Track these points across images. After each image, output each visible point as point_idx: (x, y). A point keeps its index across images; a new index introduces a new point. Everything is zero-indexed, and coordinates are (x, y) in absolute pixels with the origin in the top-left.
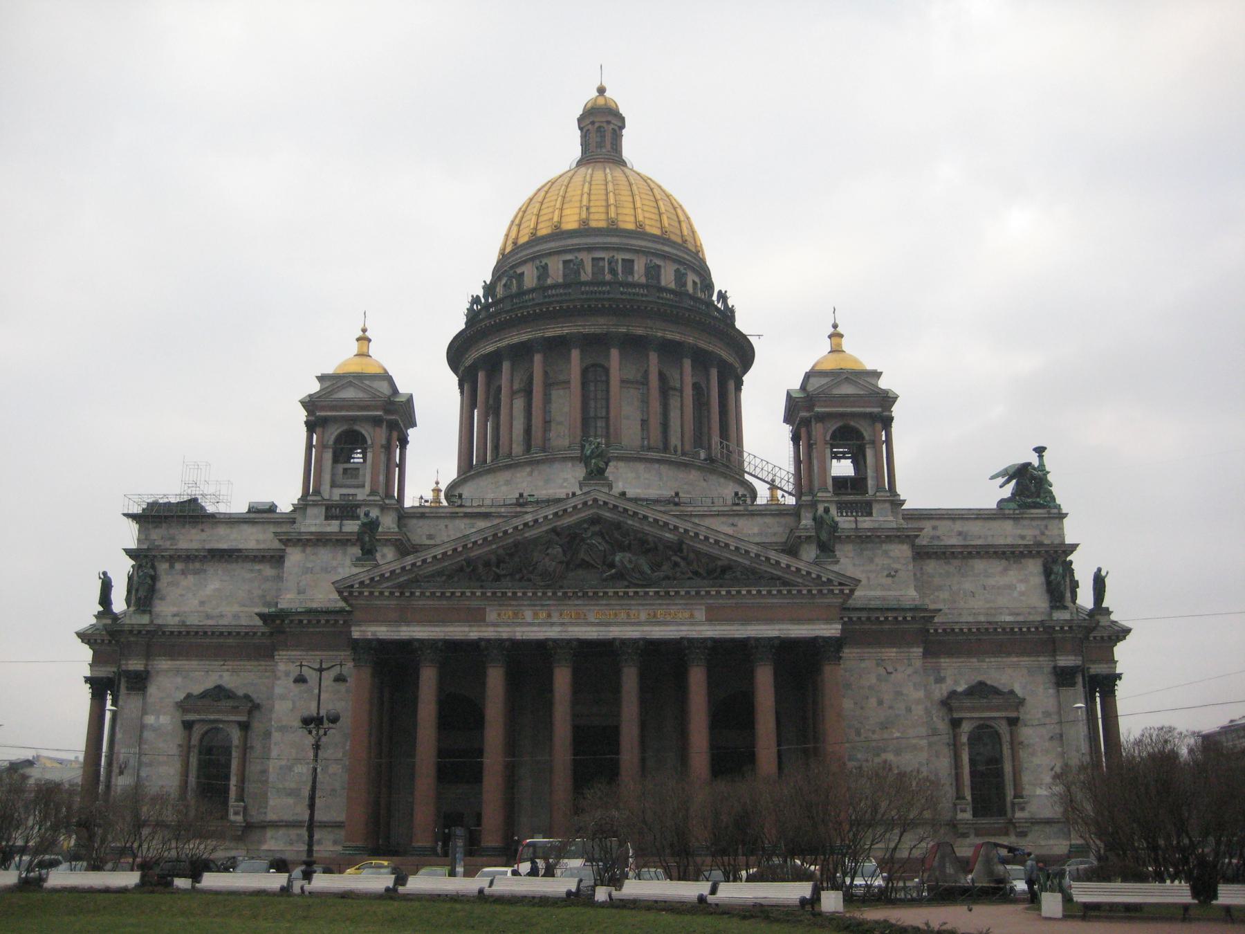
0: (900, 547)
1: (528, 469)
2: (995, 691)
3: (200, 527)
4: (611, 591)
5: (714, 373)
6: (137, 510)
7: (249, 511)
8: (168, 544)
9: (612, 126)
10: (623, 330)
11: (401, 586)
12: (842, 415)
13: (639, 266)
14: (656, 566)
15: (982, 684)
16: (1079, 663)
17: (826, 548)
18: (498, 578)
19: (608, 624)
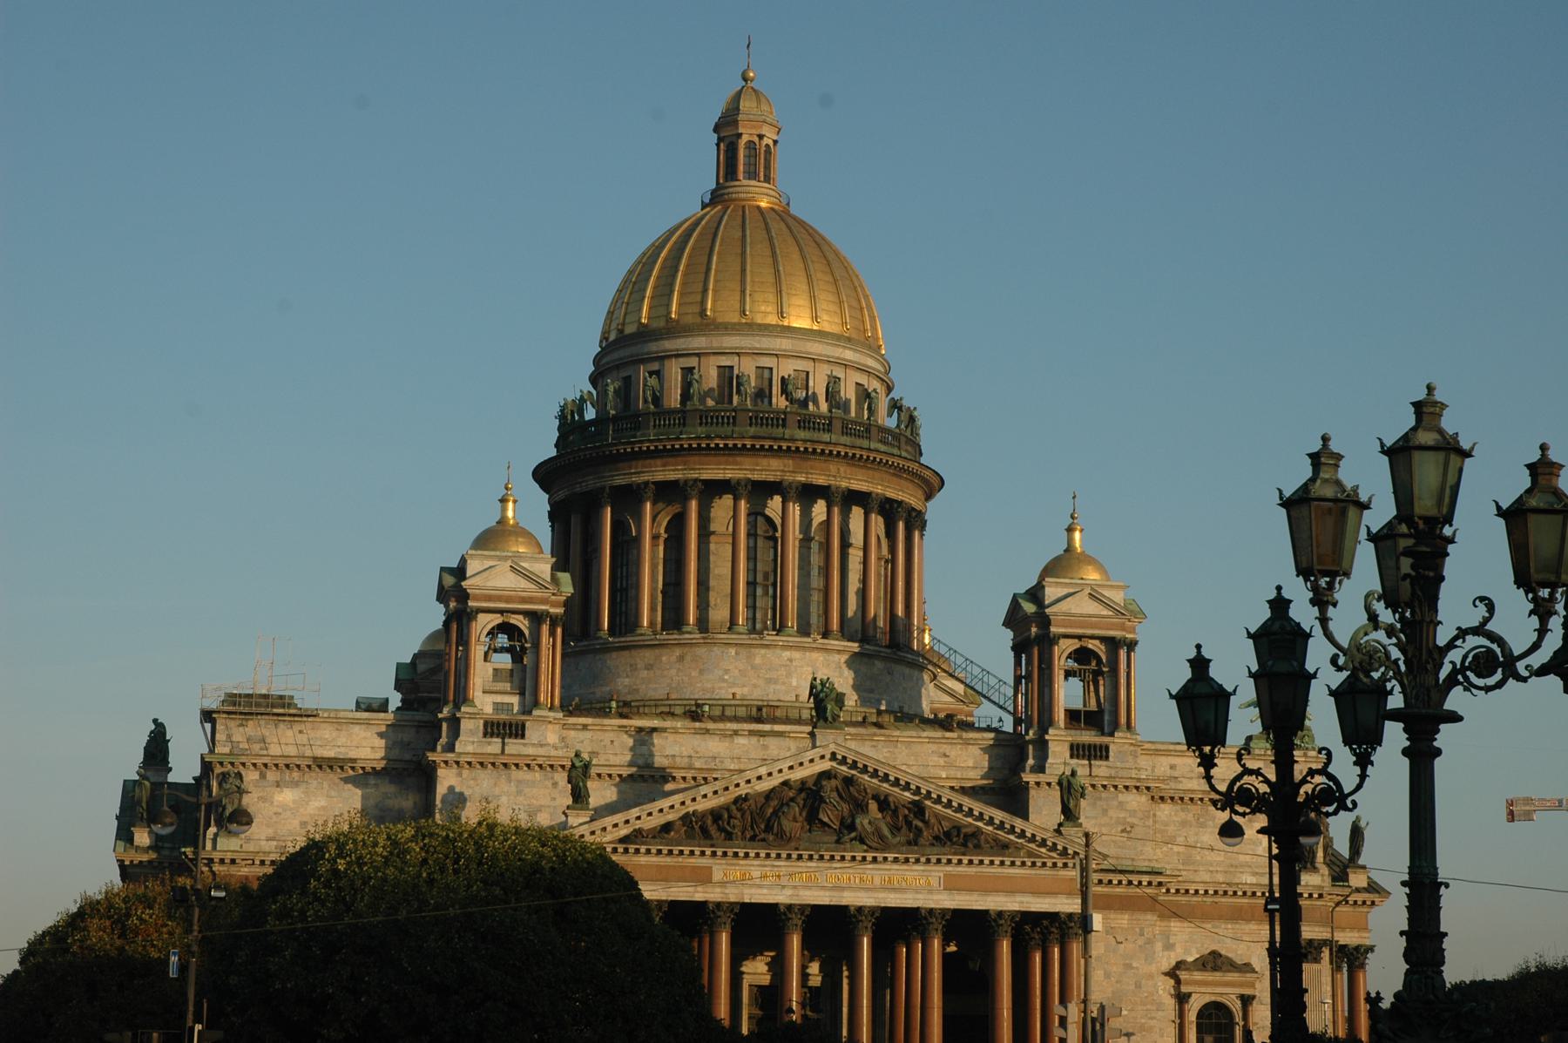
0: (1138, 798)
1: (678, 652)
2: (1232, 966)
3: (297, 727)
4: (848, 855)
5: (901, 525)
6: (214, 706)
7: (358, 707)
8: (256, 747)
9: (765, 141)
10: (801, 478)
11: (623, 840)
12: (1080, 637)
13: (819, 386)
14: (895, 829)
15: (1215, 954)
16: (1326, 935)
17: (1069, 814)
18: (729, 836)
19: (843, 889)
